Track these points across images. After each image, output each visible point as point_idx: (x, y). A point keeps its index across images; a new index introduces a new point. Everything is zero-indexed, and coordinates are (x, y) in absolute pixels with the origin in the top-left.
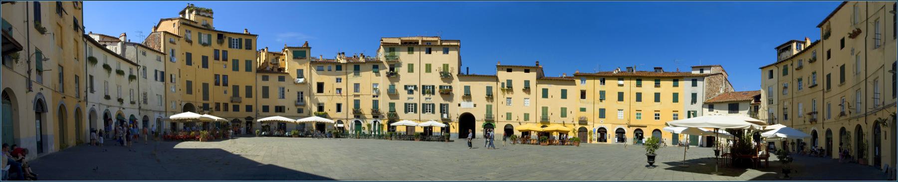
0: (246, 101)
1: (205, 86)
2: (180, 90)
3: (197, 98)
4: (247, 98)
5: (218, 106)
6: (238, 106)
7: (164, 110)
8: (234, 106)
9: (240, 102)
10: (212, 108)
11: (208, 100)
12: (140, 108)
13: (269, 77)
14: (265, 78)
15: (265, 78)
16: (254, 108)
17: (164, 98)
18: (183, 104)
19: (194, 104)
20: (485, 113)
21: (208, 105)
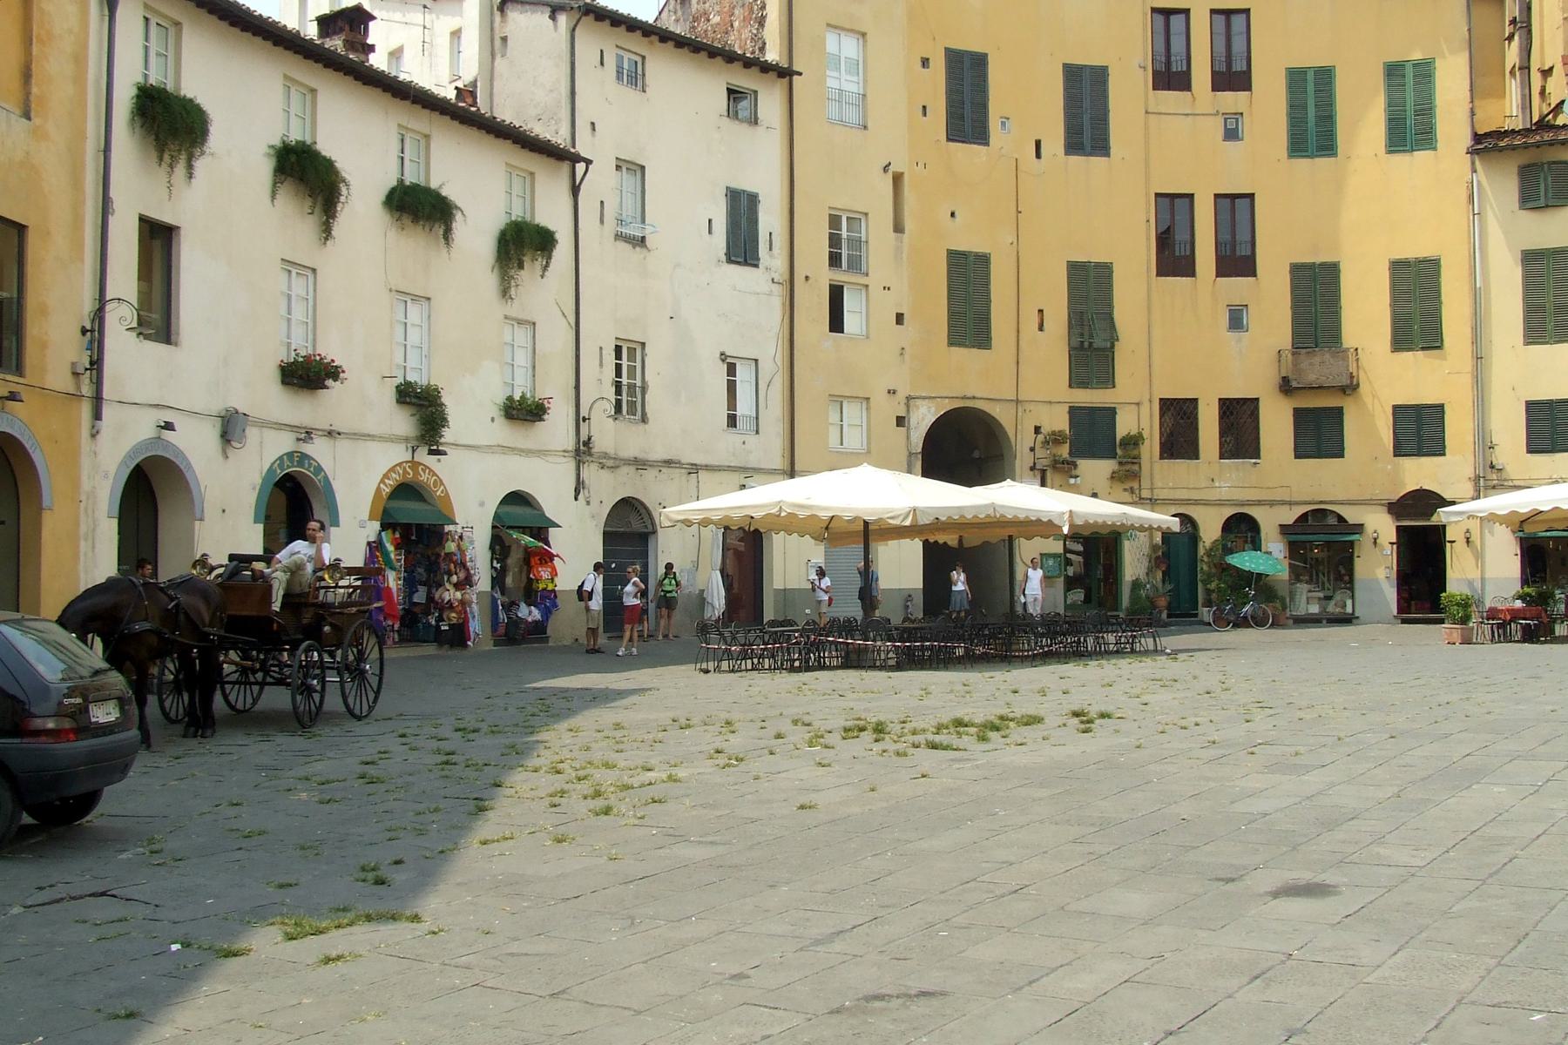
2: (900, 319)
6: (1338, 413)
8: (1299, 414)
9: (1350, 388)
10: (1134, 441)
12: (583, 451)
16: (1458, 428)
18: (924, 417)
19: (1002, 414)
21: (1111, 412)
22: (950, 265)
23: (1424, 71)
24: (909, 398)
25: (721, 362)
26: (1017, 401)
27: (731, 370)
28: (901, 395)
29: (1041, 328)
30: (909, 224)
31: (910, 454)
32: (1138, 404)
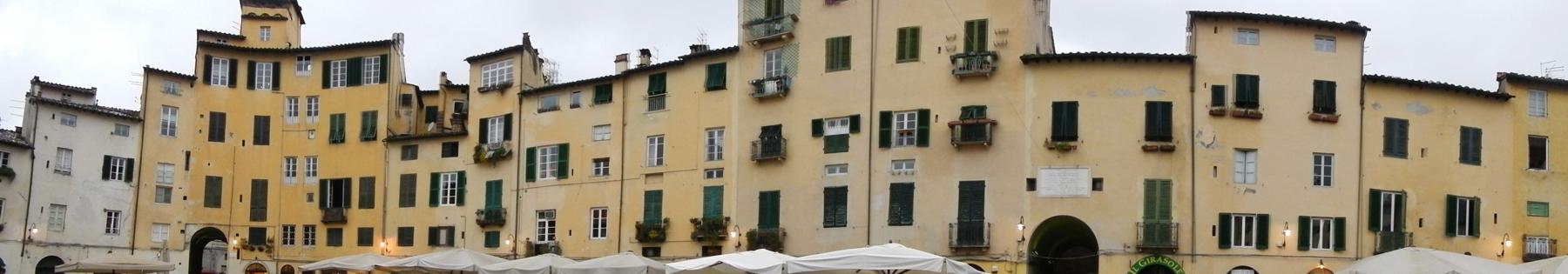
0: (357, 217)
1: (260, 188)
2: (185, 198)
3: (235, 217)
4: (363, 210)
5: (288, 233)
6: (341, 230)
7: (127, 245)
8: (329, 231)
11: (264, 218)
13: (419, 150)
14: (410, 153)
15: (410, 153)
17: (131, 219)
18: (192, 231)
20: (1140, 215)
21: (263, 230)
22: (206, 180)
23: (374, 114)
24: (186, 224)
25: (103, 213)
26: (230, 225)
27: (110, 214)
28: (184, 222)
29: (241, 201)
30: (191, 167)
31: (186, 243)
32: (274, 227)
